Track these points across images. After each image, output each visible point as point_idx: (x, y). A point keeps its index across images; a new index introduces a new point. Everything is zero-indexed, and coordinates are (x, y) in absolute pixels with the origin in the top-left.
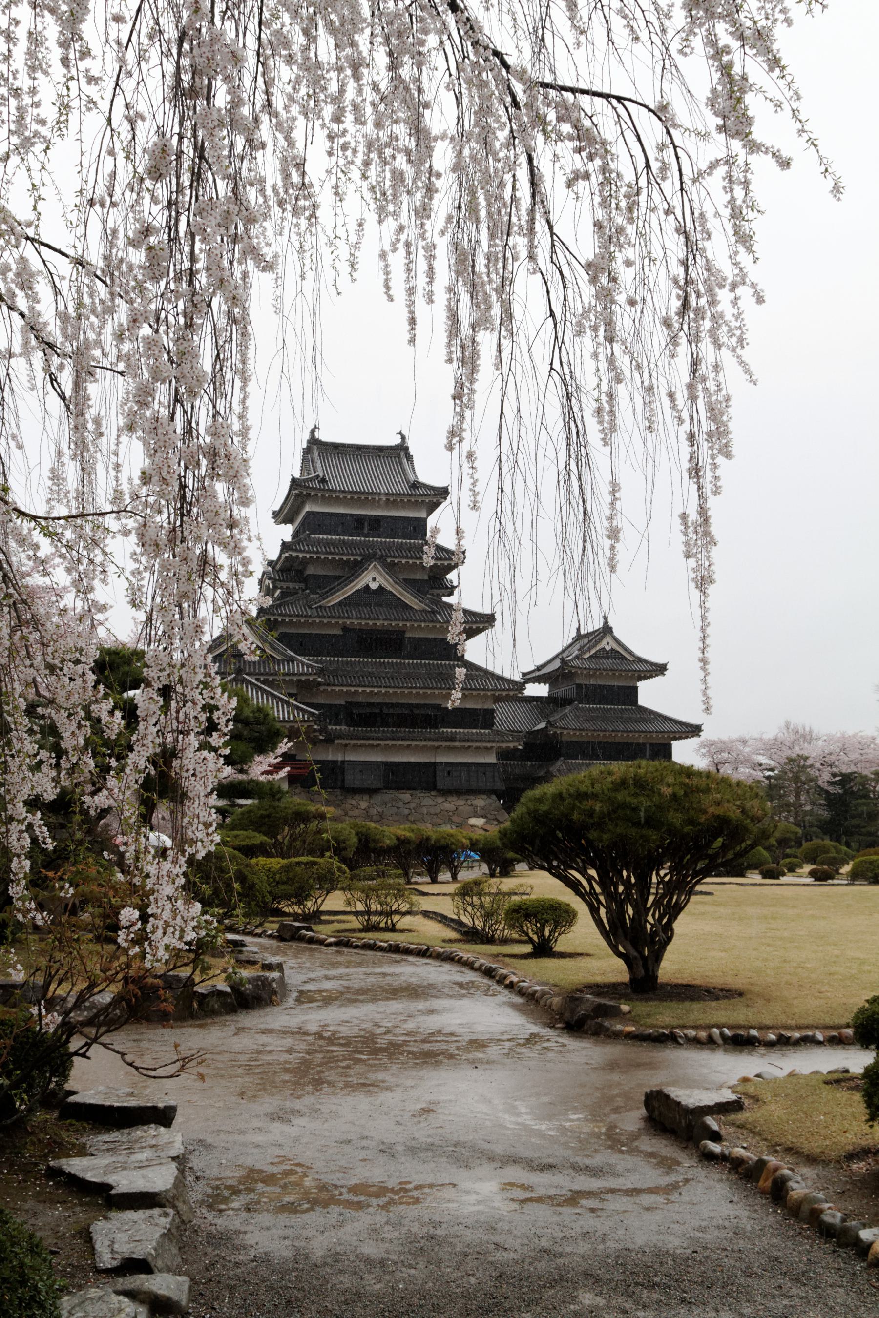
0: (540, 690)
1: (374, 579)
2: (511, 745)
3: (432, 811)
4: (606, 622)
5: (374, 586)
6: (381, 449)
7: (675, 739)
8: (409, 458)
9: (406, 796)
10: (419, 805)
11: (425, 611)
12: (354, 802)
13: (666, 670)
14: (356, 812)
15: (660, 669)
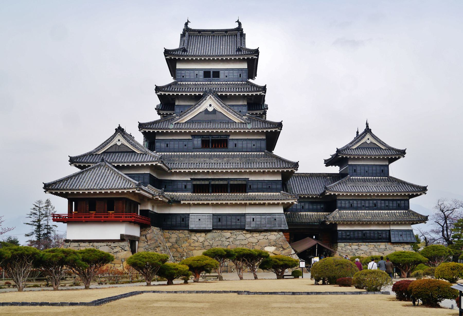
0: (335, 170)
1: (210, 105)
2: (290, 202)
3: (243, 243)
4: (367, 126)
5: (210, 109)
6: (226, 31)
7: (413, 196)
8: (243, 35)
9: (227, 234)
10: (235, 239)
11: (241, 123)
12: (195, 238)
13: (405, 153)
14: (197, 244)
15: (402, 153)
